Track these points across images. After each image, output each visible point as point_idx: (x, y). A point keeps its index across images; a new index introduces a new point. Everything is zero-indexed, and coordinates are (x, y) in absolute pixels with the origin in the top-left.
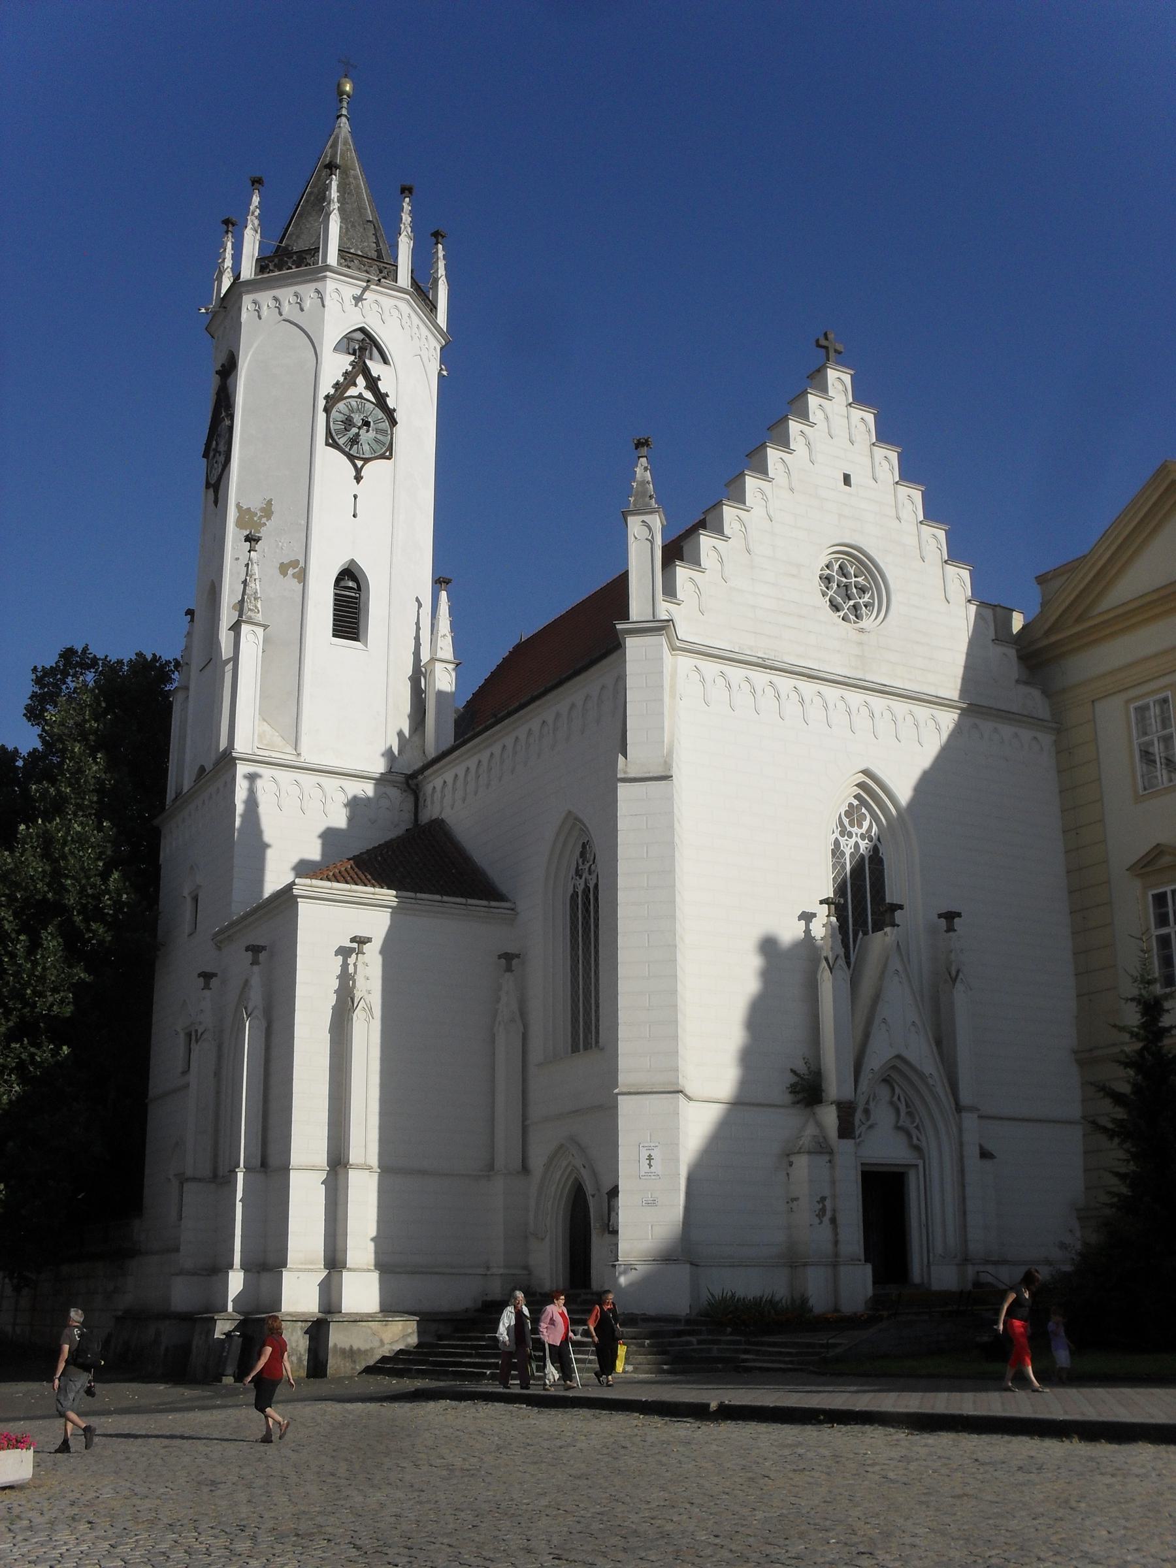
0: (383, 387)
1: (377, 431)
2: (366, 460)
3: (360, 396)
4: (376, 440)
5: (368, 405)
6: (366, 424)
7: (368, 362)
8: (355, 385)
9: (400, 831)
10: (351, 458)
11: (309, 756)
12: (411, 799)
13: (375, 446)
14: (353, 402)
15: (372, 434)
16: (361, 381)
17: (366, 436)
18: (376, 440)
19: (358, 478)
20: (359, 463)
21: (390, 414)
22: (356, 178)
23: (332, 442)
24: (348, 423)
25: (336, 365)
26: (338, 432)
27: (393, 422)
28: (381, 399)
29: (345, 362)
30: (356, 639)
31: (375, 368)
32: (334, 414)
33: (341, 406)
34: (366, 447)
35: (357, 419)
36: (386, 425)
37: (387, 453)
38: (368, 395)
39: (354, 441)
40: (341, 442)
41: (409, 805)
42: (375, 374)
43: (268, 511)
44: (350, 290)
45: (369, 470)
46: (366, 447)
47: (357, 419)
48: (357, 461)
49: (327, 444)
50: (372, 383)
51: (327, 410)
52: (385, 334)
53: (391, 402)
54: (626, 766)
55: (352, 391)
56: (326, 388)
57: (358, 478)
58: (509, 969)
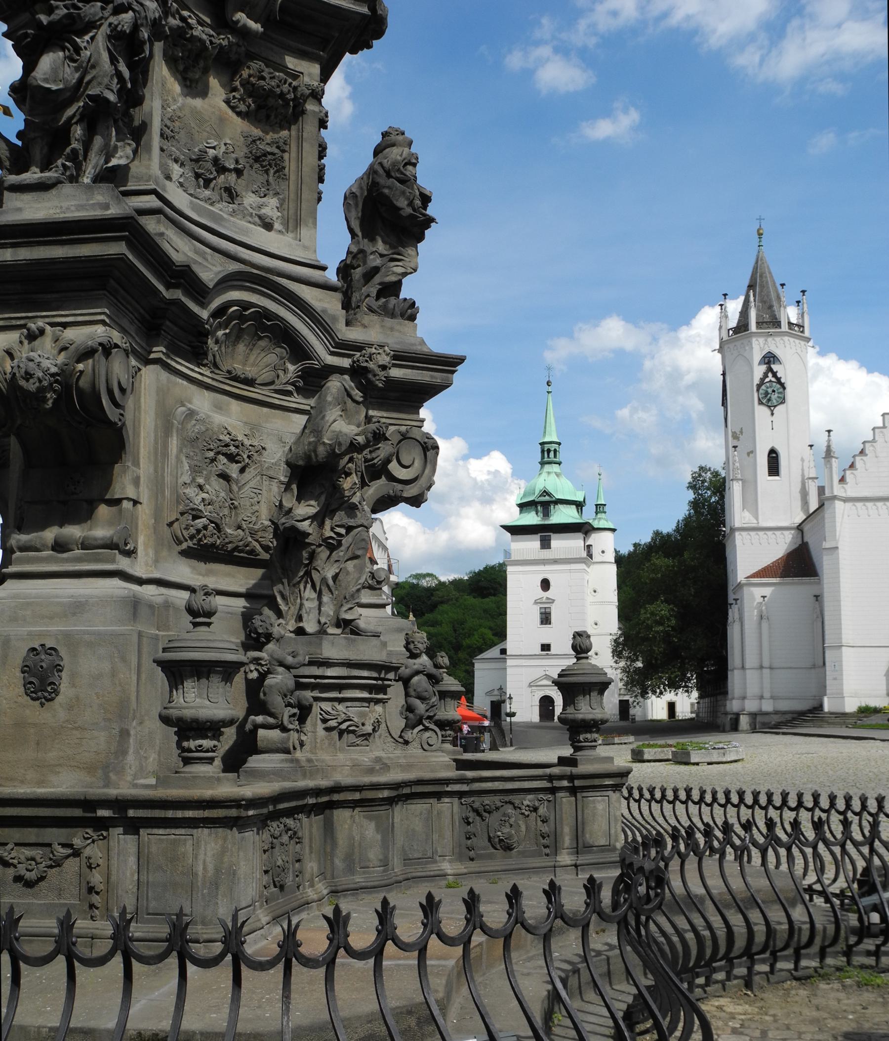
0: (779, 375)
1: (778, 393)
2: (775, 406)
3: (770, 381)
4: (778, 397)
5: (774, 384)
6: (774, 391)
7: (772, 366)
8: (768, 377)
9: (797, 546)
10: (769, 407)
11: (763, 524)
12: (801, 533)
13: (778, 399)
14: (768, 384)
15: (776, 395)
16: (770, 375)
17: (774, 397)
18: (778, 397)
19: (772, 414)
20: (772, 408)
21: (783, 386)
22: (766, 277)
23: (760, 403)
24: (767, 393)
25: (759, 371)
26: (762, 398)
27: (784, 388)
28: (779, 380)
29: (764, 368)
30: (778, 475)
31: (775, 367)
32: (761, 391)
33: (763, 387)
34: (774, 401)
35: (770, 390)
36: (781, 390)
37: (783, 401)
38: (773, 379)
39: (769, 400)
40: (764, 401)
41: (800, 535)
42: (775, 370)
43: (741, 432)
44: (761, 340)
45: (776, 410)
46: (774, 401)
47: (770, 390)
48: (771, 407)
49: (759, 404)
50: (775, 374)
51: (758, 390)
52: (778, 352)
53: (783, 381)
54: (826, 545)
55: (767, 380)
56: (757, 381)
57: (772, 414)
58: (817, 600)
